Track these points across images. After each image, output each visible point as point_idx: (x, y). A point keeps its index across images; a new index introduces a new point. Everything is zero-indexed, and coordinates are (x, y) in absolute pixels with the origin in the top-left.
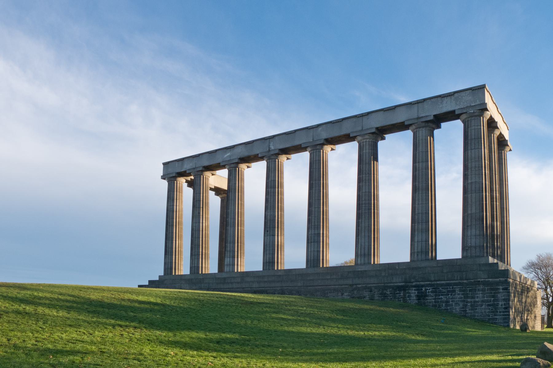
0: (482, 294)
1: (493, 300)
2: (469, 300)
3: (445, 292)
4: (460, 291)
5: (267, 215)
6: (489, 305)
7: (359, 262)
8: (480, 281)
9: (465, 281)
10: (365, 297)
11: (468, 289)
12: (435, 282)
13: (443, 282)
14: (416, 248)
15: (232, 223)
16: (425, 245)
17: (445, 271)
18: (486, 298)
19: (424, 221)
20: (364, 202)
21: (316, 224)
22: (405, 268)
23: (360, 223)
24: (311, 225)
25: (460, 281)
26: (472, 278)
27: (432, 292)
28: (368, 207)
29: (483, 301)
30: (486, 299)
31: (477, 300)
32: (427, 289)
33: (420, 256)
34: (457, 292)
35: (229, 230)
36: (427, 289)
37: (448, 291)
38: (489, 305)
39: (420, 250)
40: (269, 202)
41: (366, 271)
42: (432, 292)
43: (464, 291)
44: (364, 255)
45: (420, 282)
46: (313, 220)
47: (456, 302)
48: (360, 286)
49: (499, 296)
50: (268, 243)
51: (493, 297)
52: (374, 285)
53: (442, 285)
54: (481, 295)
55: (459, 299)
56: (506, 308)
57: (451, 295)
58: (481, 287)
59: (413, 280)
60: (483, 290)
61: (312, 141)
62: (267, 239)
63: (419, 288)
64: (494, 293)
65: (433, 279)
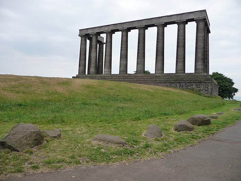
6: (205, 91)
14: (178, 68)
27: (185, 85)
29: (203, 89)
33: (179, 71)
38: (205, 91)
43: (196, 85)
51: (207, 88)
53: (188, 82)
56: (211, 92)
65: (185, 80)
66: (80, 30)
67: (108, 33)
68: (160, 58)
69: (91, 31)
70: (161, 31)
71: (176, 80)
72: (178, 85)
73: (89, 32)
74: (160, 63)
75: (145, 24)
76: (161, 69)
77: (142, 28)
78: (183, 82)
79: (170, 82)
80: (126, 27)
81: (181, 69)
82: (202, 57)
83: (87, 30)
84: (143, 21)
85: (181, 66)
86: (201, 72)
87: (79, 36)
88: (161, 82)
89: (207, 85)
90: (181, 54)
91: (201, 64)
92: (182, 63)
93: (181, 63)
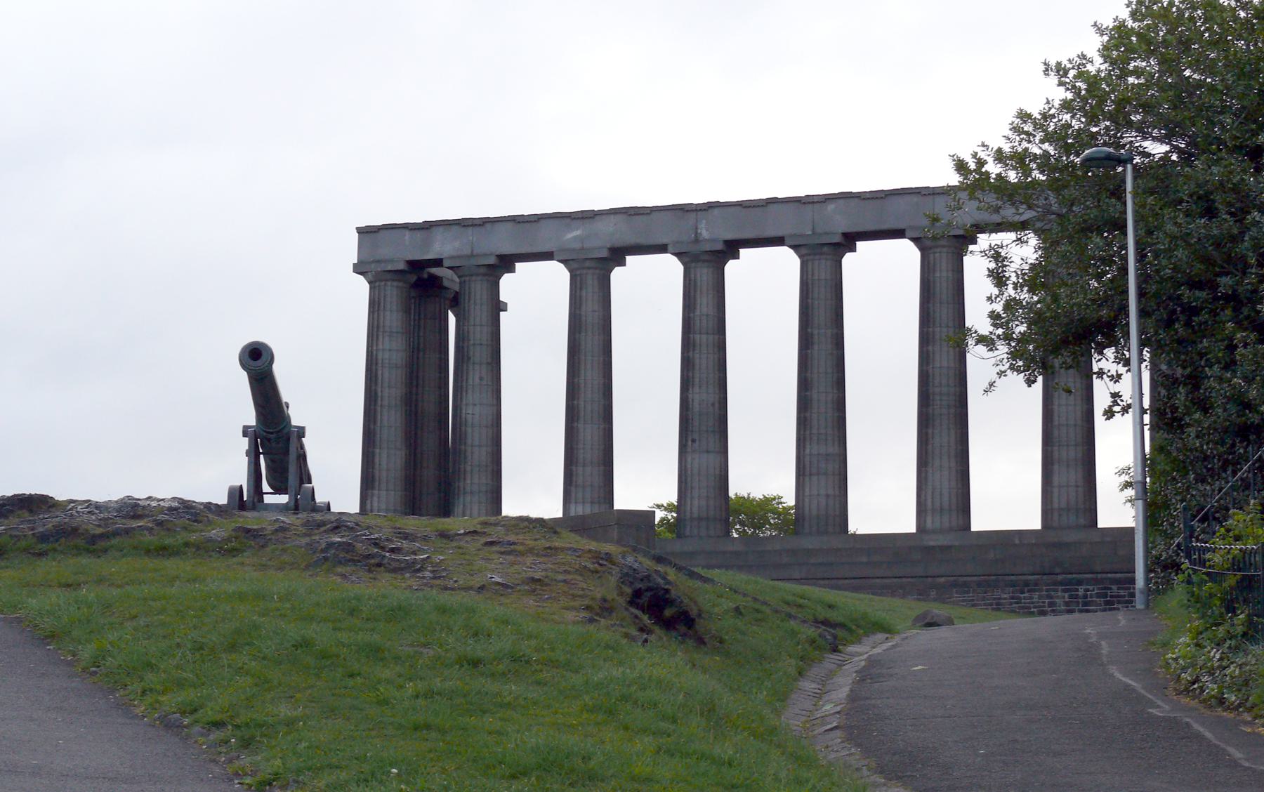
3: (1124, 596)
5: (693, 400)
7: (929, 524)
12: (1104, 575)
13: (1118, 575)
14: (1056, 500)
16: (1074, 494)
19: (1073, 443)
22: (1033, 542)
23: (930, 436)
24: (811, 434)
27: (1098, 595)
32: (1088, 590)
35: (581, 430)
36: (1088, 590)
39: (1063, 505)
40: (697, 367)
41: (949, 547)
42: (1098, 595)
44: (941, 509)
46: (815, 423)
48: (942, 580)
50: (695, 471)
52: (975, 578)
59: (1057, 570)
61: (810, 233)
62: (693, 459)
63: (1070, 585)
65: (1098, 568)
66: (361, 231)
67: (587, 264)
69: (457, 244)
70: (943, 274)
71: (1047, 571)
72: (1061, 597)
73: (441, 247)
74: (946, 473)
75: (841, 223)
77: (825, 249)
78: (1088, 582)
79: (1013, 584)
80: (712, 233)
83: (419, 235)
84: (831, 207)
87: (359, 269)
88: (965, 584)
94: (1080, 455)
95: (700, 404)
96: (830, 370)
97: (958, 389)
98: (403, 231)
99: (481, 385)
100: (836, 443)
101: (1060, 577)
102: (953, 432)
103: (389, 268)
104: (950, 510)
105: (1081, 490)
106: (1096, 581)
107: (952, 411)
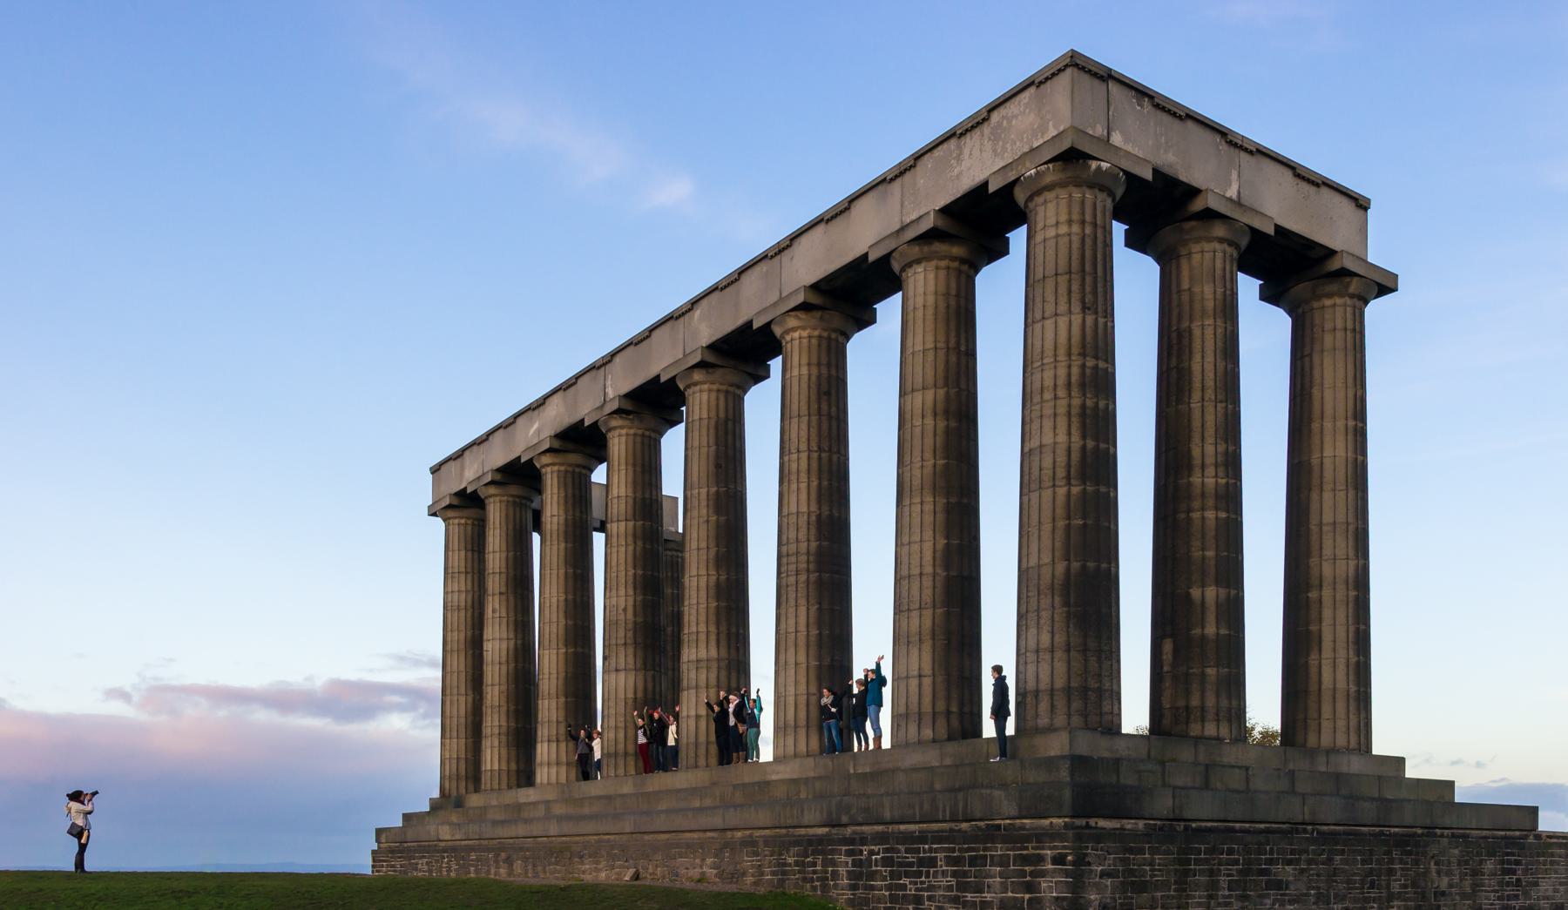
0: (1000, 877)
1: (1028, 900)
2: (969, 896)
3: (911, 864)
4: (951, 861)
8: (999, 826)
9: (964, 826)
10: (744, 874)
11: (966, 855)
15: (547, 636)
17: (938, 786)
18: (1012, 892)
20: (793, 548)
21: (694, 629)
25: (953, 825)
26: (978, 815)
28: (795, 566)
30: (1010, 894)
31: (988, 896)
34: (941, 866)
37: (921, 862)
45: (861, 824)
47: (939, 902)
49: (1043, 885)
51: (1030, 888)
53: (907, 838)
54: (998, 879)
55: (944, 890)
57: (928, 876)
58: (999, 850)
60: (1003, 861)
64: (1032, 874)
65: (887, 815)
68: (792, 621)
76: (802, 722)
81: (914, 707)
82: (1060, 567)
85: (914, 683)
86: (1043, 721)
89: (1025, 860)
90: (916, 561)
91: (1045, 639)
92: (927, 647)
93: (915, 652)
94: (928, 623)
95: (610, 612)
96: (703, 545)
97: (814, 545)
98: (449, 463)
99: (493, 618)
100: (713, 643)
101: (849, 830)
102: (803, 610)
103: (444, 505)
104: (796, 727)
105: (927, 681)
106: (881, 838)
107: (803, 578)
